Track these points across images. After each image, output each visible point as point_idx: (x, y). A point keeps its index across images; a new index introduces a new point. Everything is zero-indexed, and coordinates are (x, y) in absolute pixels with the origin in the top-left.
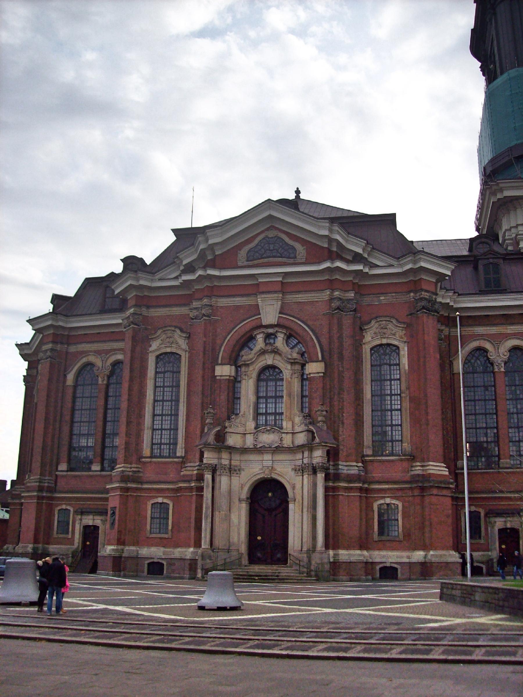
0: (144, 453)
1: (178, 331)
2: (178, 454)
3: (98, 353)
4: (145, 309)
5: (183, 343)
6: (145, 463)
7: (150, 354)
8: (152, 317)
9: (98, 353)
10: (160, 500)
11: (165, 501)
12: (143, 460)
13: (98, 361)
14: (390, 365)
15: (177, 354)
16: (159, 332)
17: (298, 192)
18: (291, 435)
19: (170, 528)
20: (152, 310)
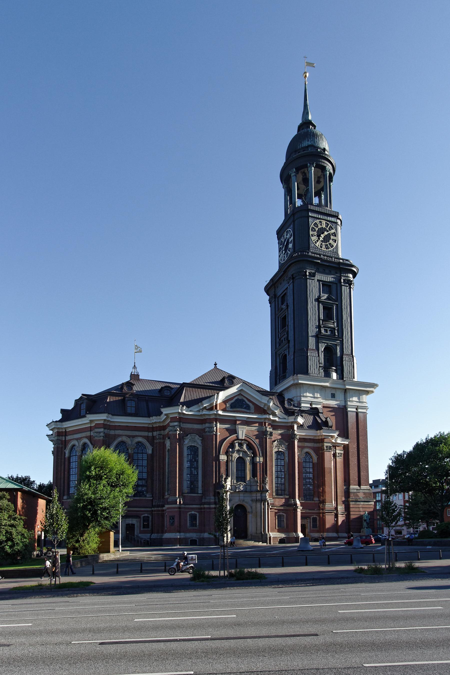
0: (184, 491)
1: (198, 436)
2: (199, 492)
3: (129, 436)
4: (181, 424)
5: (199, 442)
6: (185, 496)
7: (184, 446)
8: (184, 428)
9: (129, 436)
10: (193, 512)
11: (195, 513)
12: (185, 494)
13: (128, 441)
14: (281, 459)
15: (196, 447)
16: (189, 435)
17: (215, 364)
18: (250, 486)
19: (198, 524)
20: (184, 424)
